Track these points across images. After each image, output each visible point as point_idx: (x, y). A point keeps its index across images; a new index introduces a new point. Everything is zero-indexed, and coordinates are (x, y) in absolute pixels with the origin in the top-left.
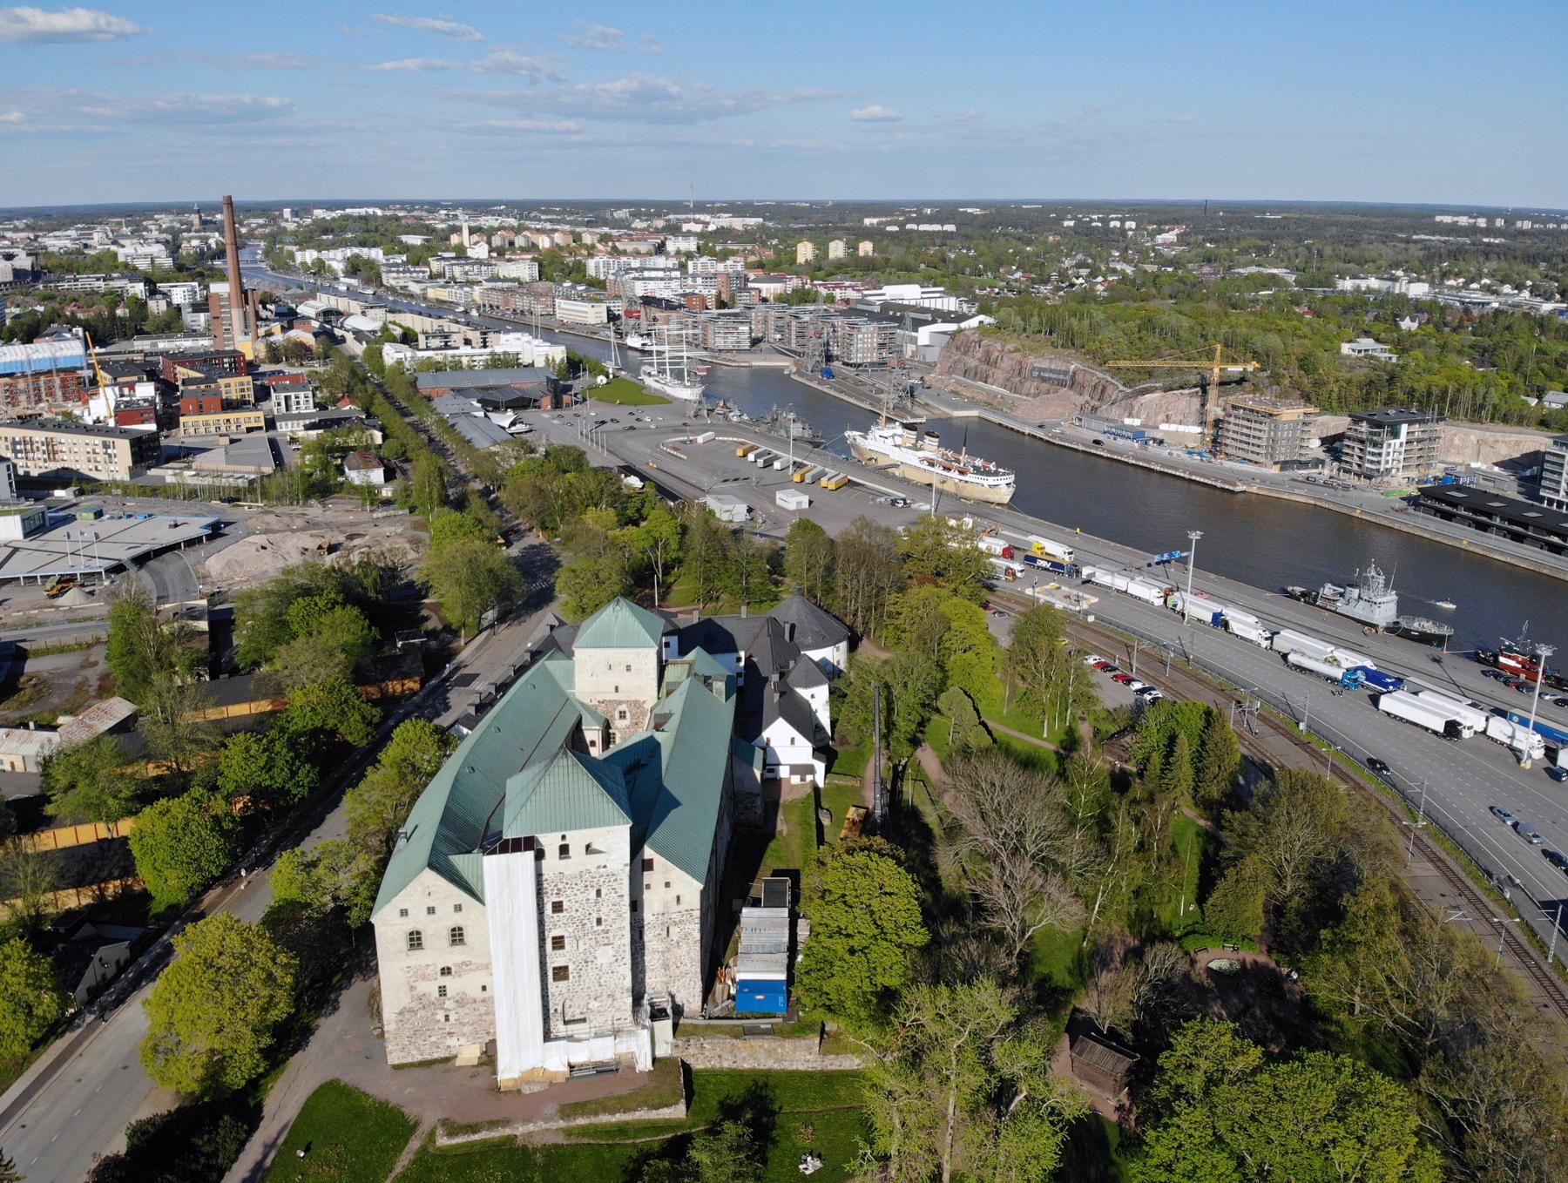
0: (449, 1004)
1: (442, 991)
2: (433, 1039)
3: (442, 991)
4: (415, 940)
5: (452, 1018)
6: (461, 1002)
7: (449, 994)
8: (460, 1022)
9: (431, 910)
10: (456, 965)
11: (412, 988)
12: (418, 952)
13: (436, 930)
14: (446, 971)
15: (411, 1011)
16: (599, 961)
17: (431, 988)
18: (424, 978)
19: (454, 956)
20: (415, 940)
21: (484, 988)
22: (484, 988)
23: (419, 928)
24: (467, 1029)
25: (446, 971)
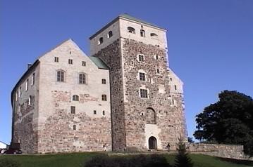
0: (76, 119)
1: (73, 109)
2: (66, 140)
3: (73, 109)
4: (61, 76)
5: (77, 128)
6: (83, 118)
7: (76, 113)
8: (81, 132)
9: (70, 62)
10: (82, 95)
11: (57, 105)
12: (62, 84)
13: (72, 72)
14: (76, 98)
17: (66, 107)
18: (64, 100)
19: (80, 90)
20: (61, 76)
21: (95, 112)
22: (95, 112)
23: (64, 69)
24: (85, 137)
25: (76, 98)
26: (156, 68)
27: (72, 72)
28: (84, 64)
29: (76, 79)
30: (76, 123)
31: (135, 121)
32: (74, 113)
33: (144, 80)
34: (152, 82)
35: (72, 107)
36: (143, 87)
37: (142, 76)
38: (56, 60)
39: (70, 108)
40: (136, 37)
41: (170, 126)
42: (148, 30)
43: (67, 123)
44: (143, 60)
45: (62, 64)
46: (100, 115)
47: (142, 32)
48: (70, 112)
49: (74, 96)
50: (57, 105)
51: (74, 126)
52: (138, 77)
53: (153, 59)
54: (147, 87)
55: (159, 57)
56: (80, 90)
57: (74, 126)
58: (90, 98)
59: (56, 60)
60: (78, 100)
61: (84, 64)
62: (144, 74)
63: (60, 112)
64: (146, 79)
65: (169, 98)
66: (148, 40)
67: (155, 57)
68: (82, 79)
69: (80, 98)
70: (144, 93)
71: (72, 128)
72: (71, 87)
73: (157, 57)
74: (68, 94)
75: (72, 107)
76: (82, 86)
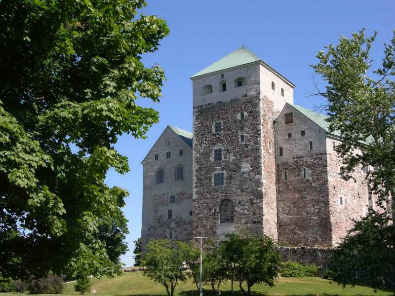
1: (170, 212)
3: (170, 212)
5: (173, 235)
9: (169, 155)
11: (156, 211)
14: (172, 199)
15: (155, 228)
16: (243, 170)
17: (163, 211)
21: (191, 213)
25: (172, 199)
26: (240, 133)
29: (173, 176)
30: (172, 229)
31: (205, 223)
32: (171, 218)
33: (220, 158)
34: (232, 158)
35: (169, 211)
37: (218, 153)
38: (157, 157)
39: (167, 212)
41: (254, 222)
43: (164, 232)
44: (220, 130)
48: (167, 218)
49: (171, 197)
50: (156, 211)
51: (171, 234)
52: (212, 159)
53: (235, 121)
54: (223, 169)
55: (245, 114)
57: (171, 234)
58: (185, 196)
60: (174, 201)
61: (181, 153)
62: (220, 150)
63: (159, 219)
64: (223, 157)
65: (257, 177)
67: (239, 117)
69: (176, 198)
70: (219, 179)
71: (169, 236)
73: (242, 115)
74: (166, 196)
75: (169, 211)
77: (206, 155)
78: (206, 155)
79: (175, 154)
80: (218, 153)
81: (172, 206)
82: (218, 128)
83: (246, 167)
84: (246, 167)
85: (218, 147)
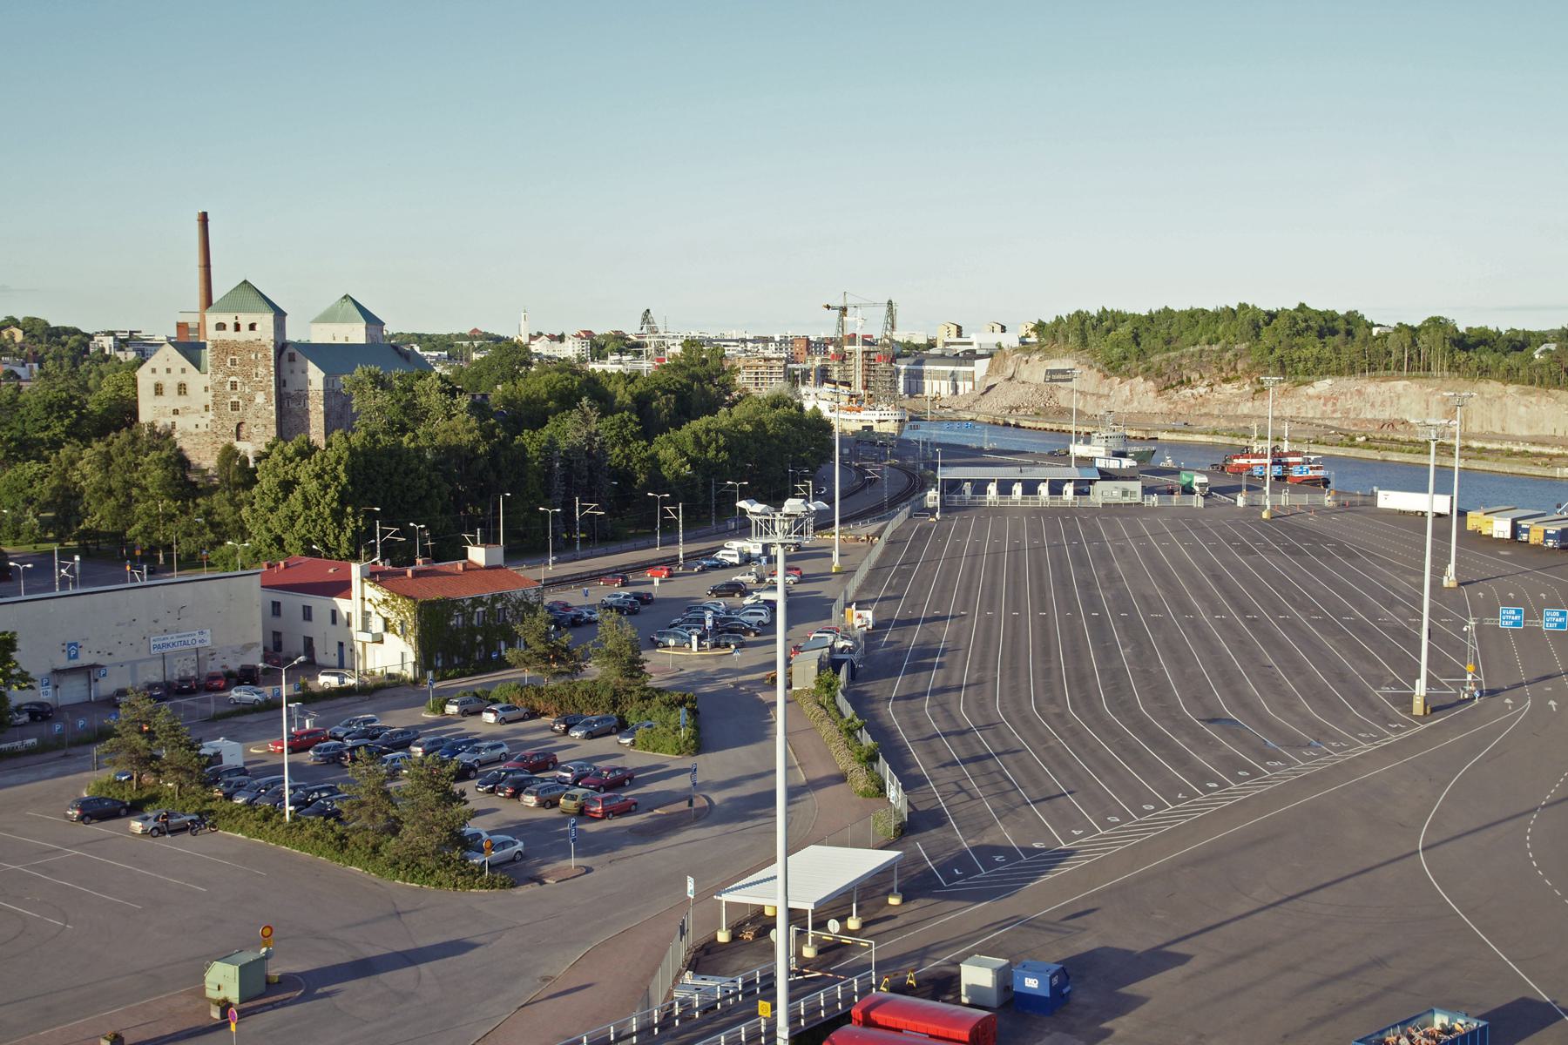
13: (170, 383)
14: (176, 412)
18: (164, 415)
19: (180, 403)
23: (161, 381)
25: (176, 412)
27: (170, 383)
28: (183, 371)
36: (235, 399)
37: (234, 385)
38: (154, 371)
40: (229, 335)
42: (245, 319)
45: (161, 376)
46: (202, 429)
47: (237, 327)
52: (228, 387)
56: (180, 403)
59: (154, 371)
61: (183, 371)
66: (245, 335)
68: (182, 389)
70: (235, 406)
72: (171, 400)
76: (183, 397)
77: (222, 384)
78: (222, 384)
79: (176, 370)
80: (234, 385)
81: (176, 418)
82: (233, 362)
83: (260, 398)
84: (260, 398)
85: (233, 379)
